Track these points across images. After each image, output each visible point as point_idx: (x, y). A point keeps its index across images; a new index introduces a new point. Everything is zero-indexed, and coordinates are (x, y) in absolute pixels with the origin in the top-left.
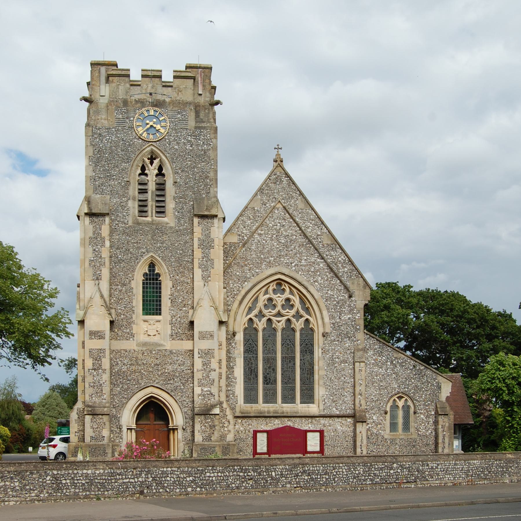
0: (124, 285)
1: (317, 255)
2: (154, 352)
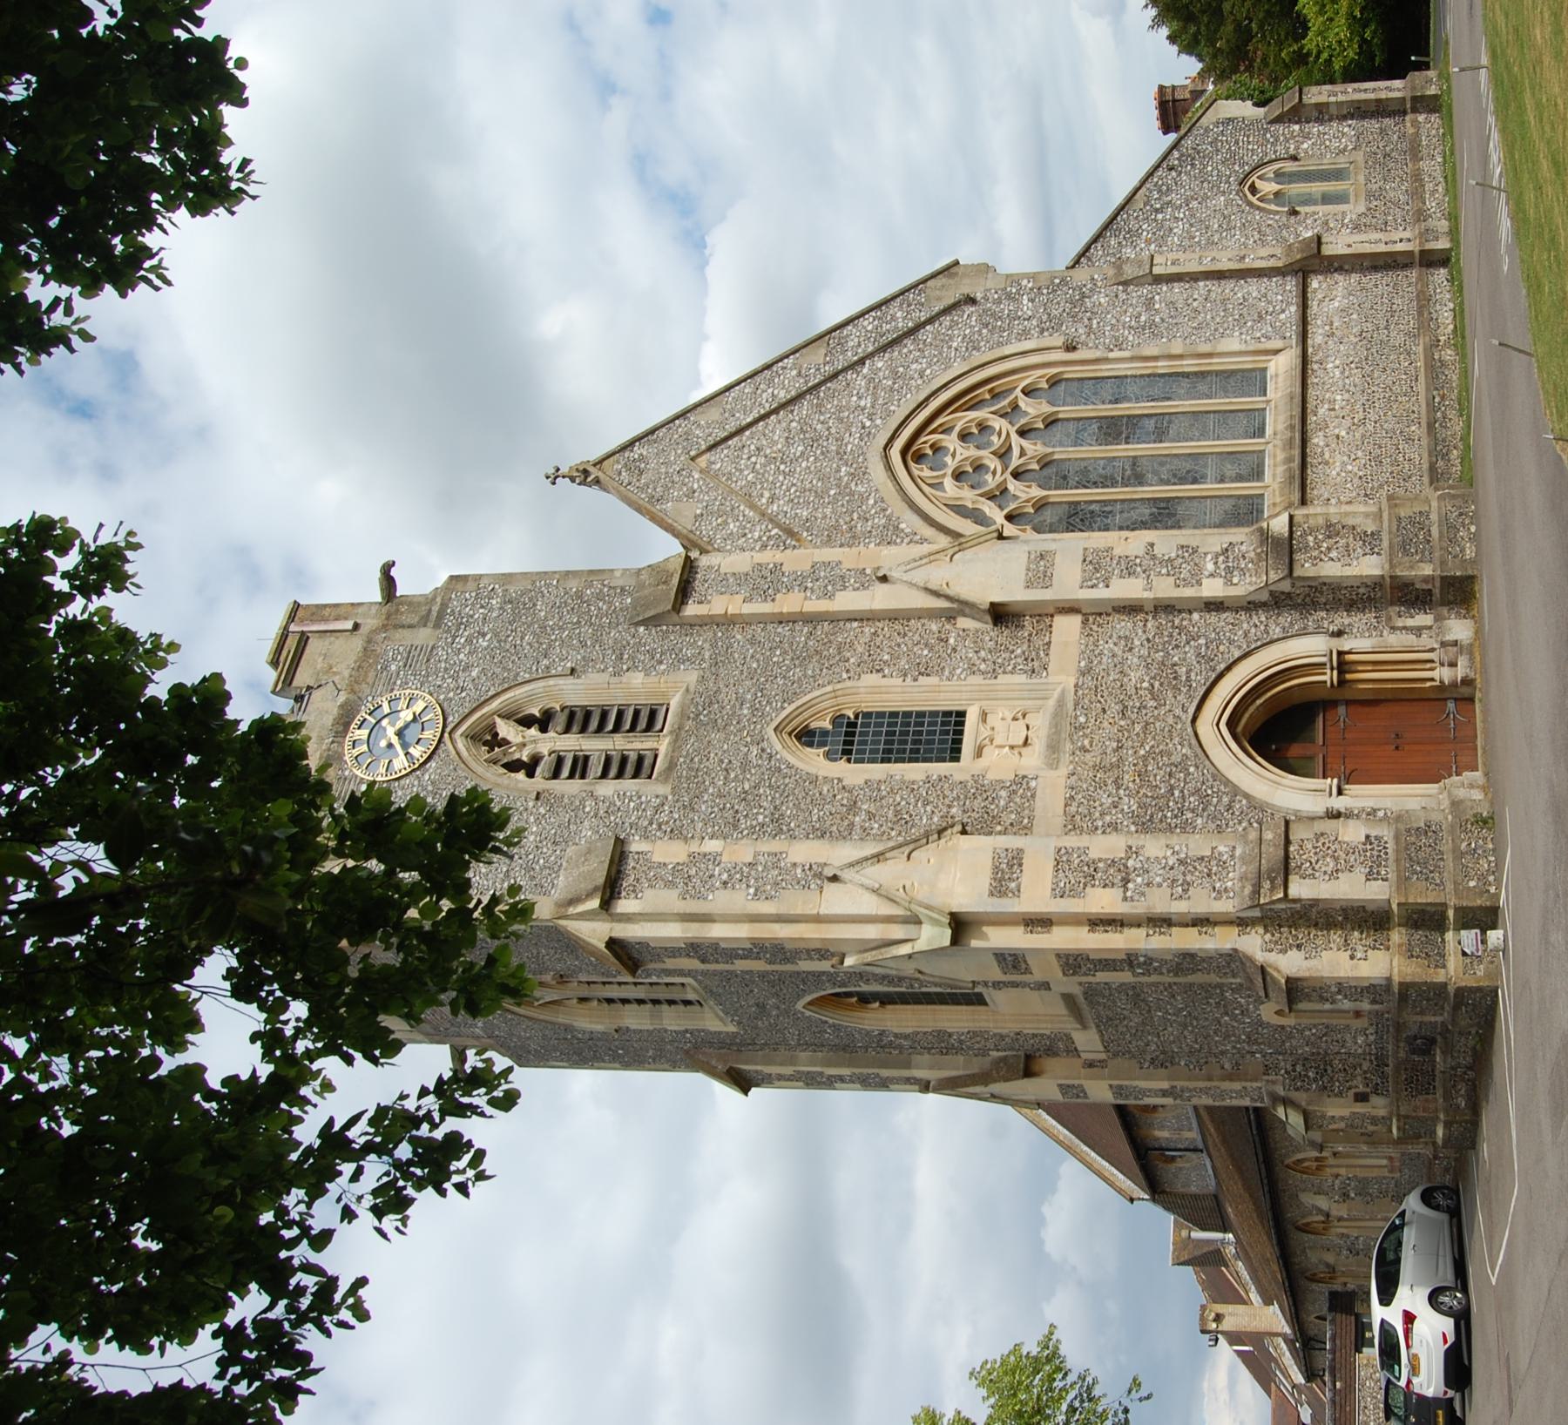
0: (853, 806)
1: (850, 375)
2: (1082, 719)
